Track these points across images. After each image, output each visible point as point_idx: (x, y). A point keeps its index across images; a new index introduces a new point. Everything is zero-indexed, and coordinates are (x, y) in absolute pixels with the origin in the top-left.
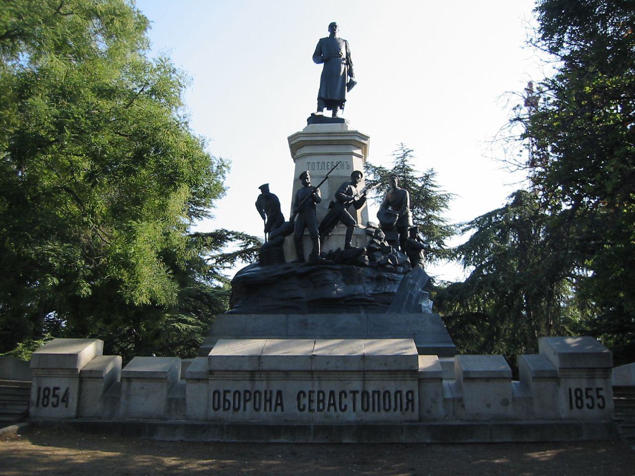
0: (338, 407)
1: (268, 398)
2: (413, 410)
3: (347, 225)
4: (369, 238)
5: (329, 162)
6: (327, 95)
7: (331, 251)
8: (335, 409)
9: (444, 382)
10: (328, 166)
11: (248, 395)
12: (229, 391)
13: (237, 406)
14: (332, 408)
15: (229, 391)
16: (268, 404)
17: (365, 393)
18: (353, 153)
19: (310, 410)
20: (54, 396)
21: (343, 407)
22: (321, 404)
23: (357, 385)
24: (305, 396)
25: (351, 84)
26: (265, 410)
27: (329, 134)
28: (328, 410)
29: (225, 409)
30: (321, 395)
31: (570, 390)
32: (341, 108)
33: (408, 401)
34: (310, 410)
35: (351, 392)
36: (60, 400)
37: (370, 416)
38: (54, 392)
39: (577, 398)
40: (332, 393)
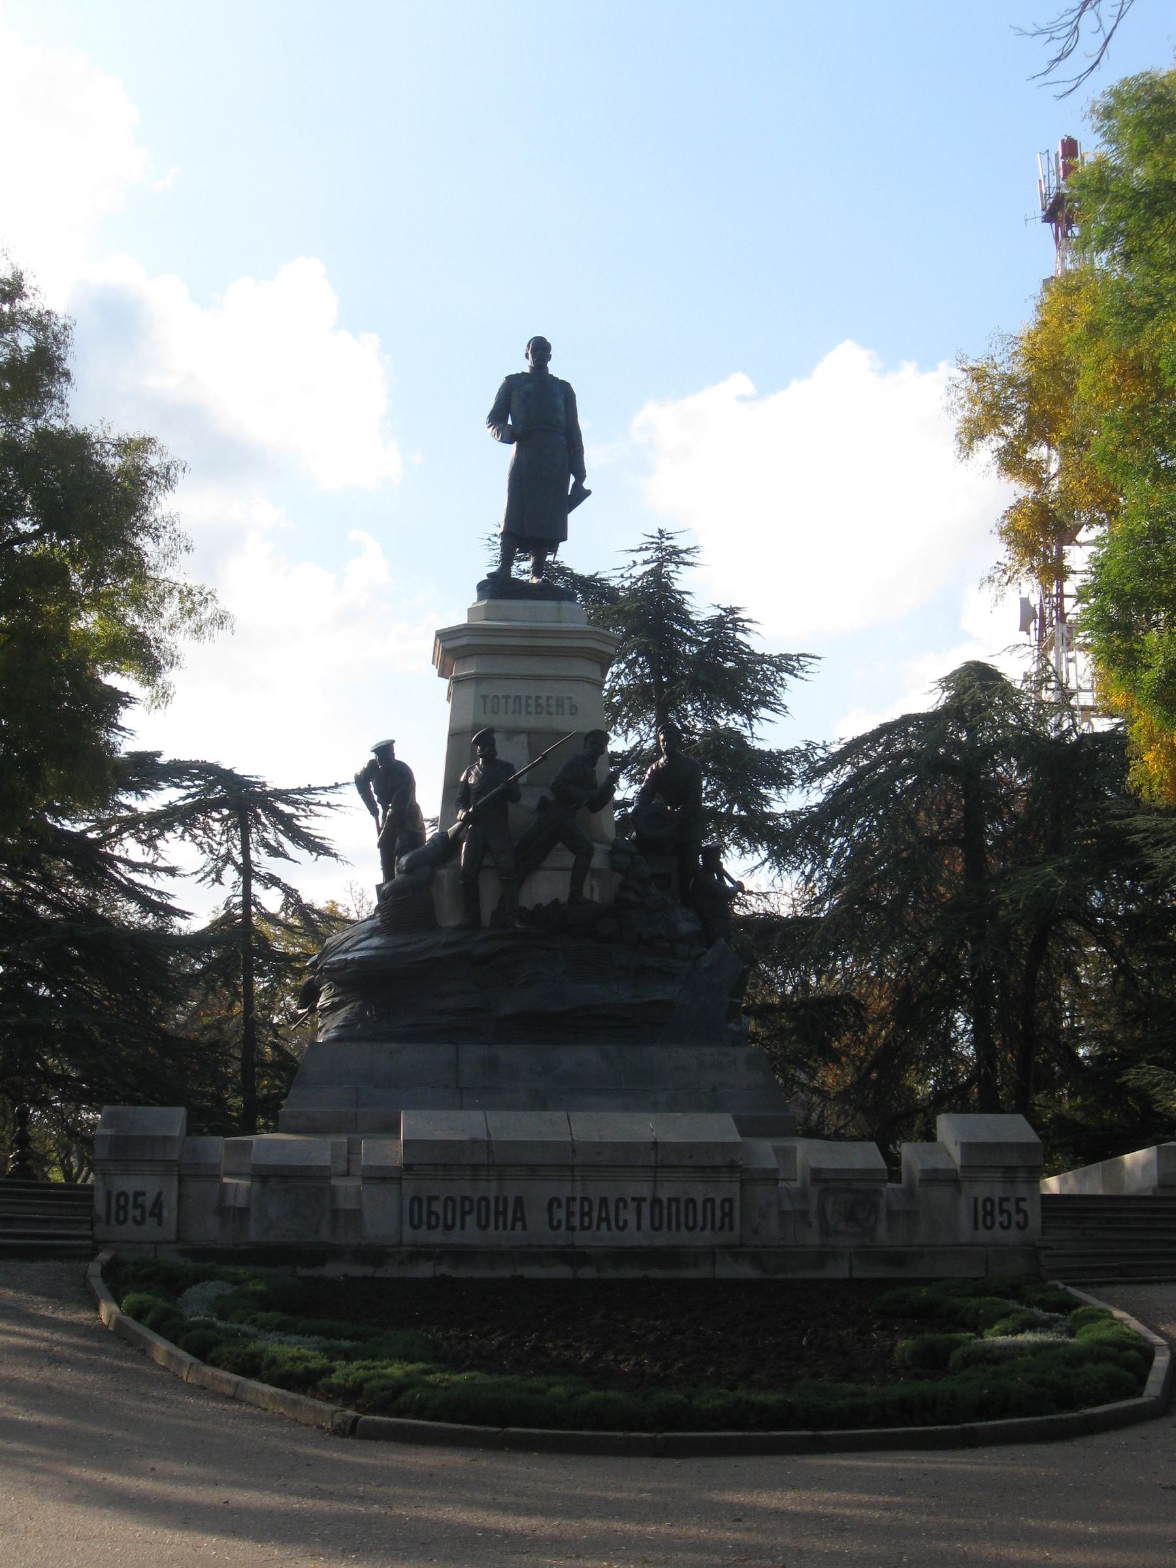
0: (613, 1223)
1: (501, 1209)
2: (731, 1229)
3: (574, 850)
4: (618, 878)
7: (539, 906)
8: (609, 1228)
9: (782, 1184)
10: (528, 705)
11: (467, 1203)
12: (437, 1198)
13: (450, 1222)
14: (604, 1225)
15: (437, 1198)
16: (501, 1219)
17: (656, 1201)
19: (570, 1228)
20: (136, 1206)
21: (621, 1224)
22: (586, 1219)
23: (643, 1189)
24: (559, 1206)
25: (581, 494)
26: (496, 1228)
28: (598, 1228)
29: (430, 1227)
30: (586, 1204)
31: (976, 1199)
33: (724, 1215)
34: (570, 1228)
35: (634, 1199)
36: (147, 1214)
37: (662, 1239)
38: (135, 1199)
39: (985, 1213)
40: (604, 1201)
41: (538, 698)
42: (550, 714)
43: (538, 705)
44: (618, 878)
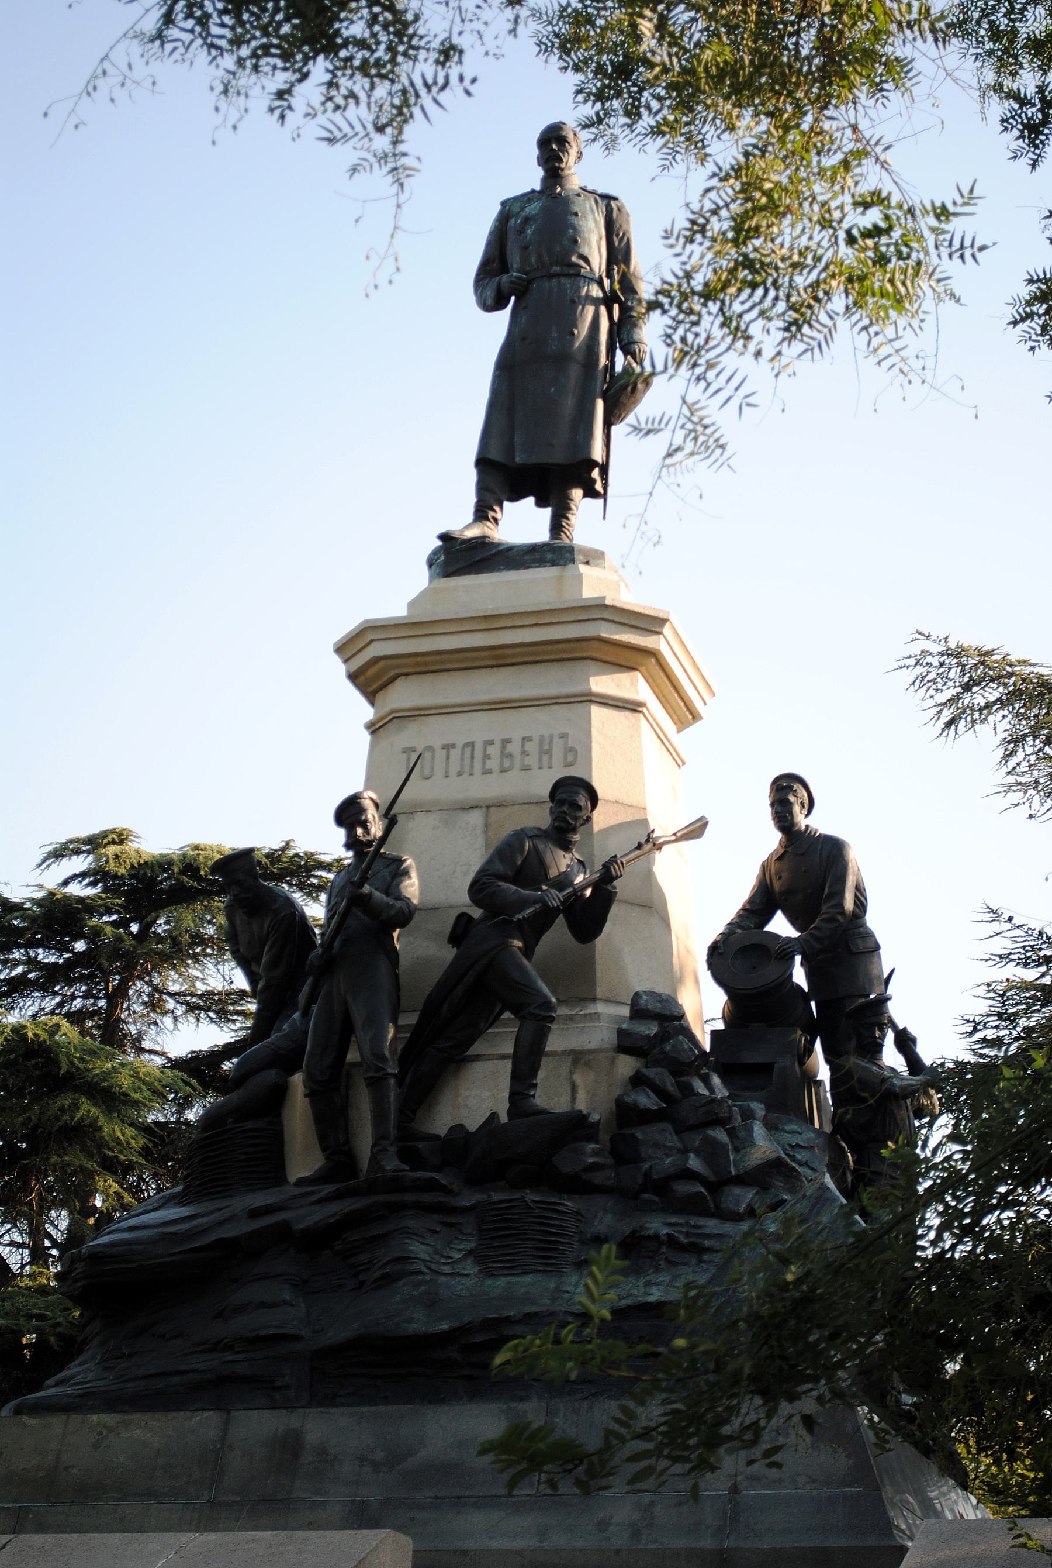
4: (626, 1066)
5: (491, 743)
6: (510, 449)
10: (486, 757)
18: (590, 694)
27: (490, 621)
32: (590, 492)
41: (506, 741)
42: (526, 769)
43: (506, 755)
44: (626, 1066)
